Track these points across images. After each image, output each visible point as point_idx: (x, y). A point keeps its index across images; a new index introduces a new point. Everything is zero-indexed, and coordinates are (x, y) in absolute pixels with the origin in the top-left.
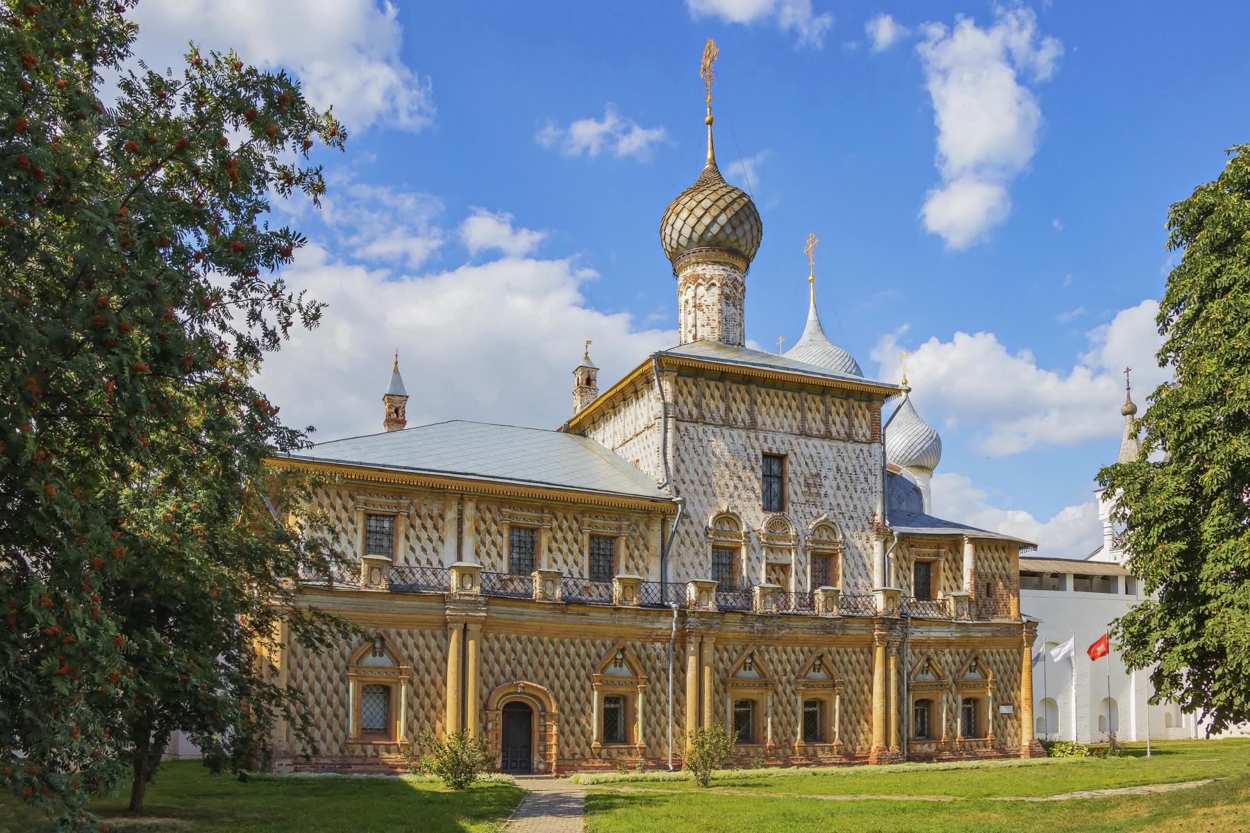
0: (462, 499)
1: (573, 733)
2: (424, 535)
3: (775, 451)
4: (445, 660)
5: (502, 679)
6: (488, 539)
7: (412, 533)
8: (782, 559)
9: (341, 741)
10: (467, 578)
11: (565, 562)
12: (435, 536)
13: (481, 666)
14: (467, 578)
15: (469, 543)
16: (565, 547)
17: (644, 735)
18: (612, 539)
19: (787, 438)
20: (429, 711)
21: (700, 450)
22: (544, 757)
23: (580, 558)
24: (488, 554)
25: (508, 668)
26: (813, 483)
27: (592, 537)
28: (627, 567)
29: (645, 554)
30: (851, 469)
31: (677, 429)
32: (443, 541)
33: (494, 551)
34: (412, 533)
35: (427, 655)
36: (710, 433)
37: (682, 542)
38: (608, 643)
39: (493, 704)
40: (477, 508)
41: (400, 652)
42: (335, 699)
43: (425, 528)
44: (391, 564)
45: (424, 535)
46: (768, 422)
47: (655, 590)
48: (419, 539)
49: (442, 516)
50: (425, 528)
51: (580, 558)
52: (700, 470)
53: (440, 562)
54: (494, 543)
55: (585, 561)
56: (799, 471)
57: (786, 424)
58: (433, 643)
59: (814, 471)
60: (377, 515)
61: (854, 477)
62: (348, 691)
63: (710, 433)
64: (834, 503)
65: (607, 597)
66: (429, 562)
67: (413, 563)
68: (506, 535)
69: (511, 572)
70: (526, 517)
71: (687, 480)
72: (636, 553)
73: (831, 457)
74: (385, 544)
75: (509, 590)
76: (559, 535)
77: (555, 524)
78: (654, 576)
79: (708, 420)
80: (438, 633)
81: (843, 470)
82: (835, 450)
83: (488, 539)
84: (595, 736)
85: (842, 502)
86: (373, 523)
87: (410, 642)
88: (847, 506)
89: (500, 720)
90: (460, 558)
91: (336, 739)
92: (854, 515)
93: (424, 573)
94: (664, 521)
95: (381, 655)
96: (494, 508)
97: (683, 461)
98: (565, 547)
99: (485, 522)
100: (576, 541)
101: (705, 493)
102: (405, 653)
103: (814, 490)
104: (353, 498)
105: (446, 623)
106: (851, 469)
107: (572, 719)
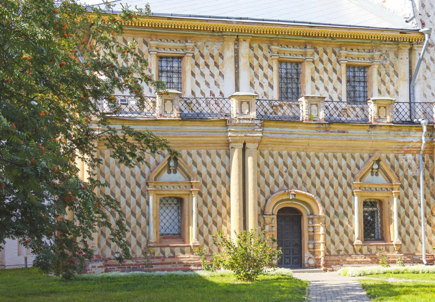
0: (237, 40)
1: (337, 233)
2: (206, 71)
4: (228, 174)
5: (276, 189)
6: (260, 73)
7: (197, 71)
9: (144, 245)
10: (245, 105)
11: (326, 89)
12: (216, 71)
13: (258, 178)
14: (245, 105)
15: (245, 75)
16: (325, 76)
17: (400, 234)
18: (365, 68)
20: (216, 217)
22: (313, 253)
23: (338, 85)
24: (261, 85)
27: (348, 66)
28: (380, 92)
29: (395, 79)
32: (223, 76)
33: (266, 84)
34: (197, 71)
35: (213, 171)
37: (428, 68)
38: (366, 156)
39: (269, 210)
40: (251, 47)
41: (190, 169)
42: (138, 211)
43: (207, 65)
44: (179, 95)
45: (206, 71)
47: (404, 109)
48: (203, 75)
49: (221, 55)
50: (207, 65)
51: (338, 85)
53: (221, 93)
54: (266, 76)
55: (343, 88)
58: (217, 161)
60: (167, 57)
62: (148, 203)
65: (363, 117)
66: (212, 94)
67: (198, 95)
68: (275, 68)
69: (281, 99)
70: (292, 53)
72: (387, 79)
74: (175, 80)
75: (280, 114)
76: (320, 67)
77: (316, 57)
78: (404, 97)
80: (222, 152)
83: (260, 73)
84: (356, 235)
86: (164, 64)
87: (199, 160)
89: (275, 223)
90: (237, 89)
91: (139, 244)
93: (207, 104)
94: (411, 50)
95: (175, 172)
96: (264, 46)
98: (325, 76)
99: (257, 58)
100: (335, 71)
102: (195, 170)
104: (146, 43)
105: (228, 143)
107: (336, 221)
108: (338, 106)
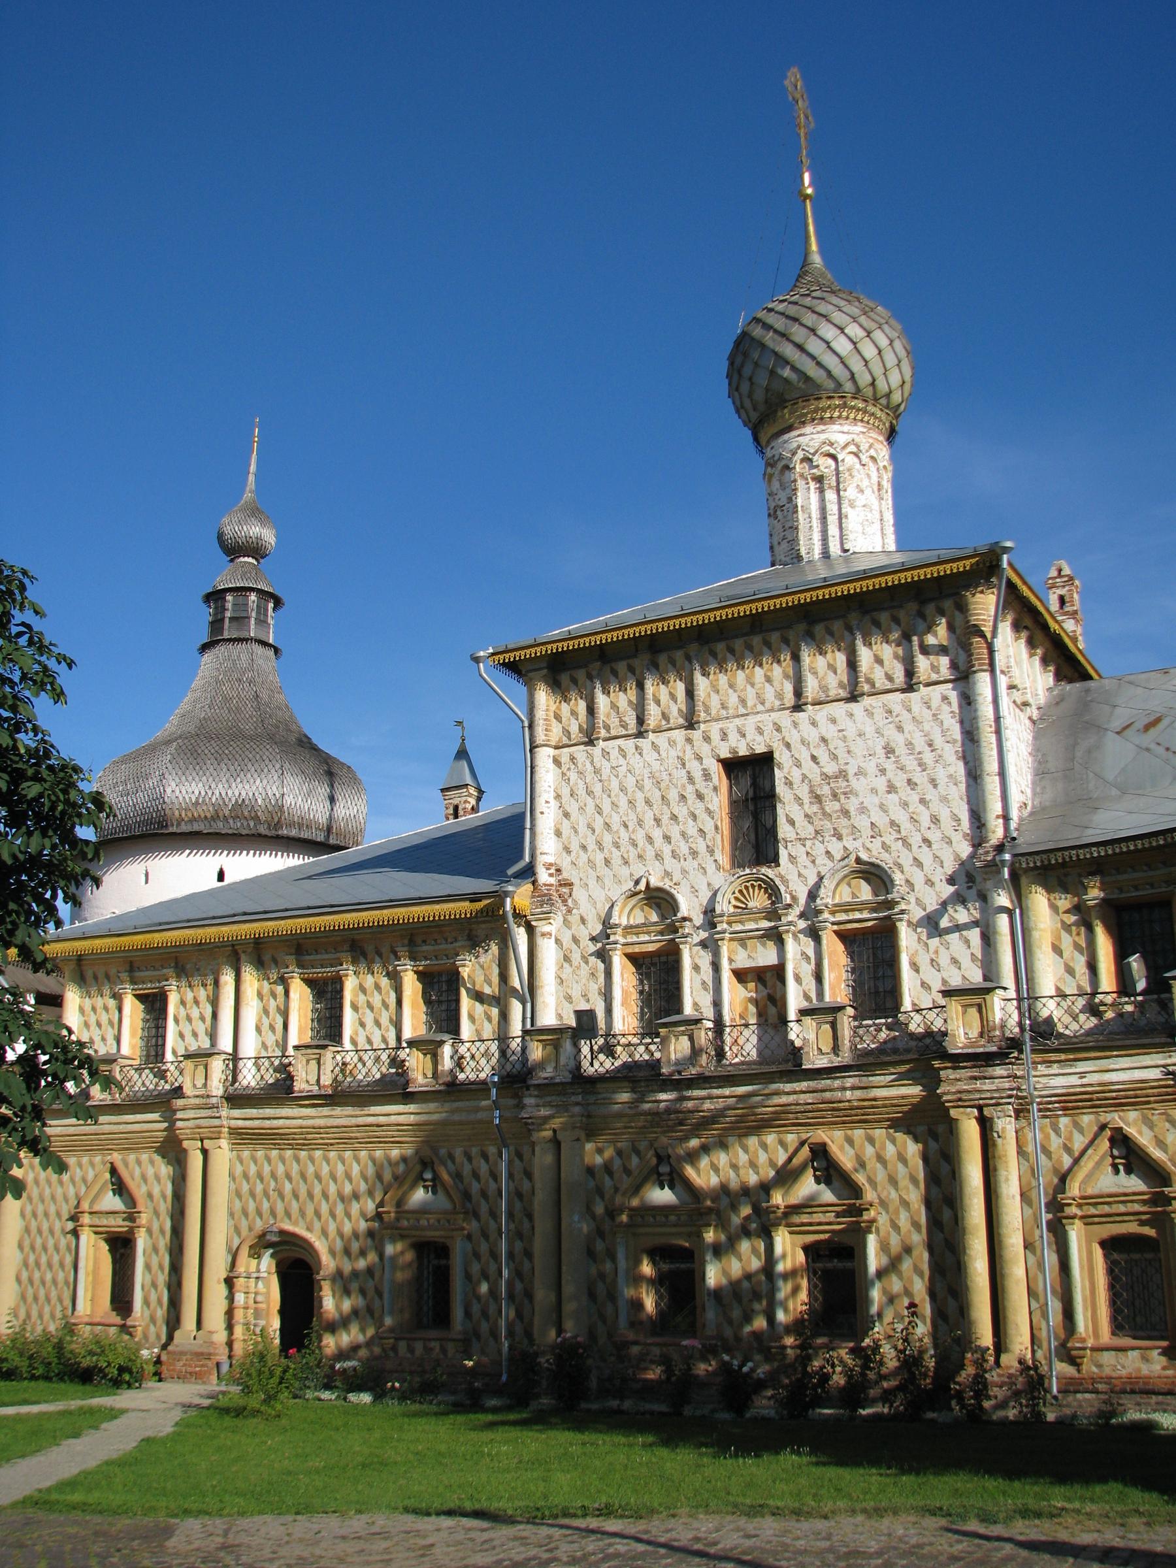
3: (743, 752)
8: (766, 956)
19: (767, 719)
21: (597, 788)
25: (295, 1205)
26: (833, 790)
30: (920, 743)
31: (557, 762)
36: (614, 753)
37: (567, 959)
46: (733, 700)
52: (599, 823)
56: (796, 775)
57: (769, 693)
59: (831, 768)
61: (928, 757)
63: (614, 753)
64: (882, 821)
71: (575, 847)
73: (869, 730)
79: (613, 733)
81: (901, 750)
82: (879, 714)
85: (901, 817)
88: (913, 820)
92: (934, 836)
97: (566, 815)
101: (607, 862)
103: (831, 806)
106: (920, 743)
108: (366, 1058)
